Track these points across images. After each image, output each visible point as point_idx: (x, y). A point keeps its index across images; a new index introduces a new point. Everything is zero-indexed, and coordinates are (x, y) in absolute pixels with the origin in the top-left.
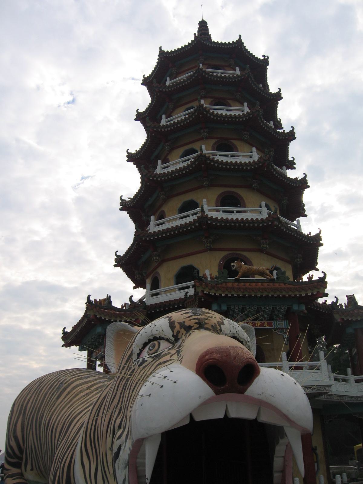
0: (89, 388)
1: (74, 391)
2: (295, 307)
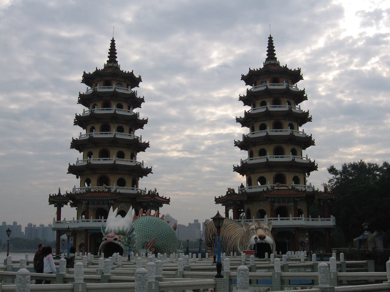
0: (233, 227)
1: (229, 228)
2: (296, 199)
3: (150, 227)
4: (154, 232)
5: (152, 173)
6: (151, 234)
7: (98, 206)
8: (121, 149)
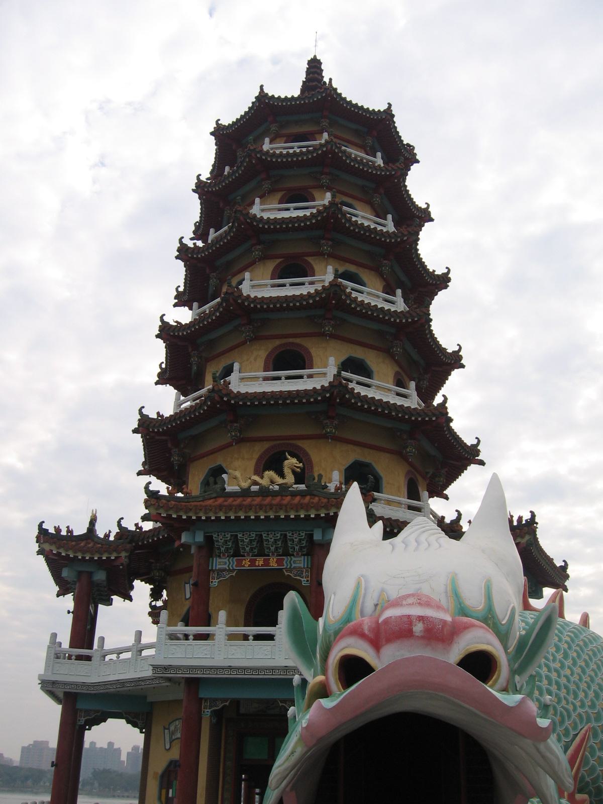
3: (552, 665)
4: (576, 696)
5: (482, 463)
6: (564, 702)
7: (260, 561)
8: (359, 353)
